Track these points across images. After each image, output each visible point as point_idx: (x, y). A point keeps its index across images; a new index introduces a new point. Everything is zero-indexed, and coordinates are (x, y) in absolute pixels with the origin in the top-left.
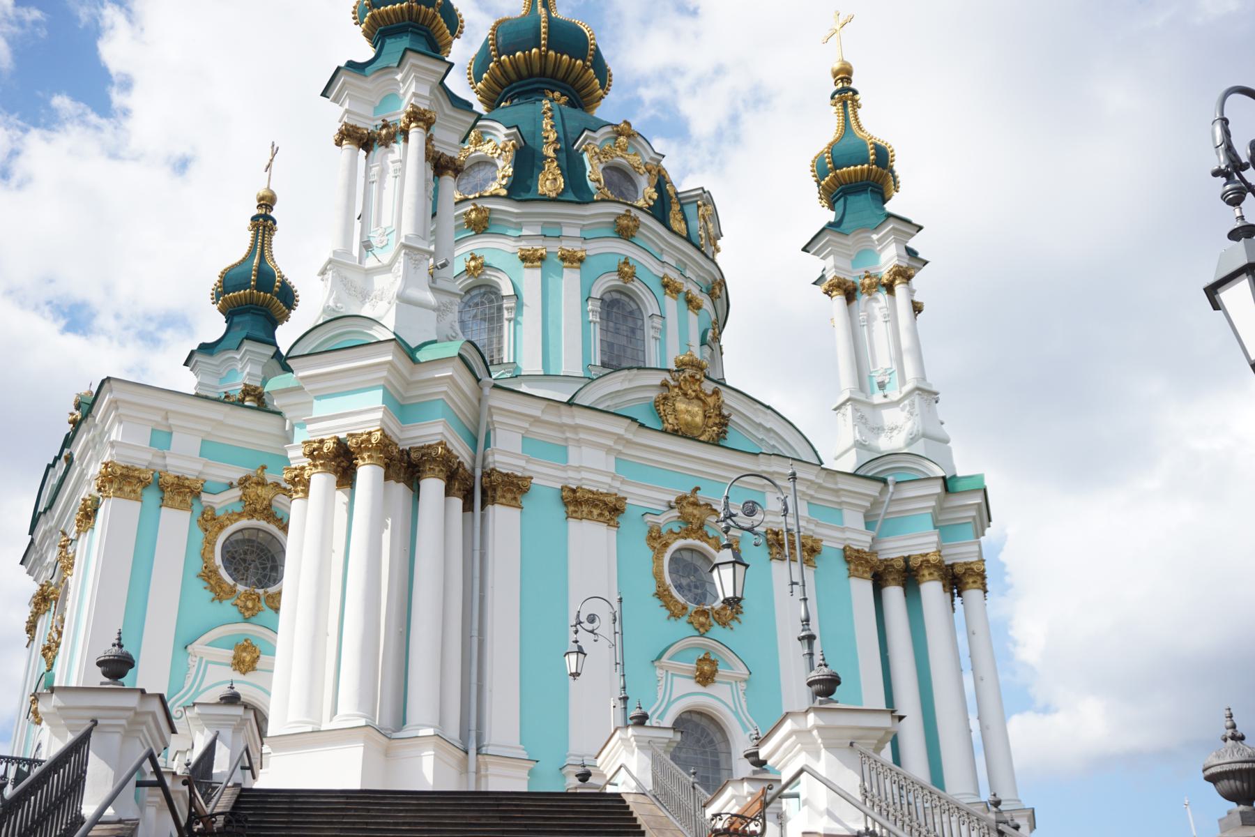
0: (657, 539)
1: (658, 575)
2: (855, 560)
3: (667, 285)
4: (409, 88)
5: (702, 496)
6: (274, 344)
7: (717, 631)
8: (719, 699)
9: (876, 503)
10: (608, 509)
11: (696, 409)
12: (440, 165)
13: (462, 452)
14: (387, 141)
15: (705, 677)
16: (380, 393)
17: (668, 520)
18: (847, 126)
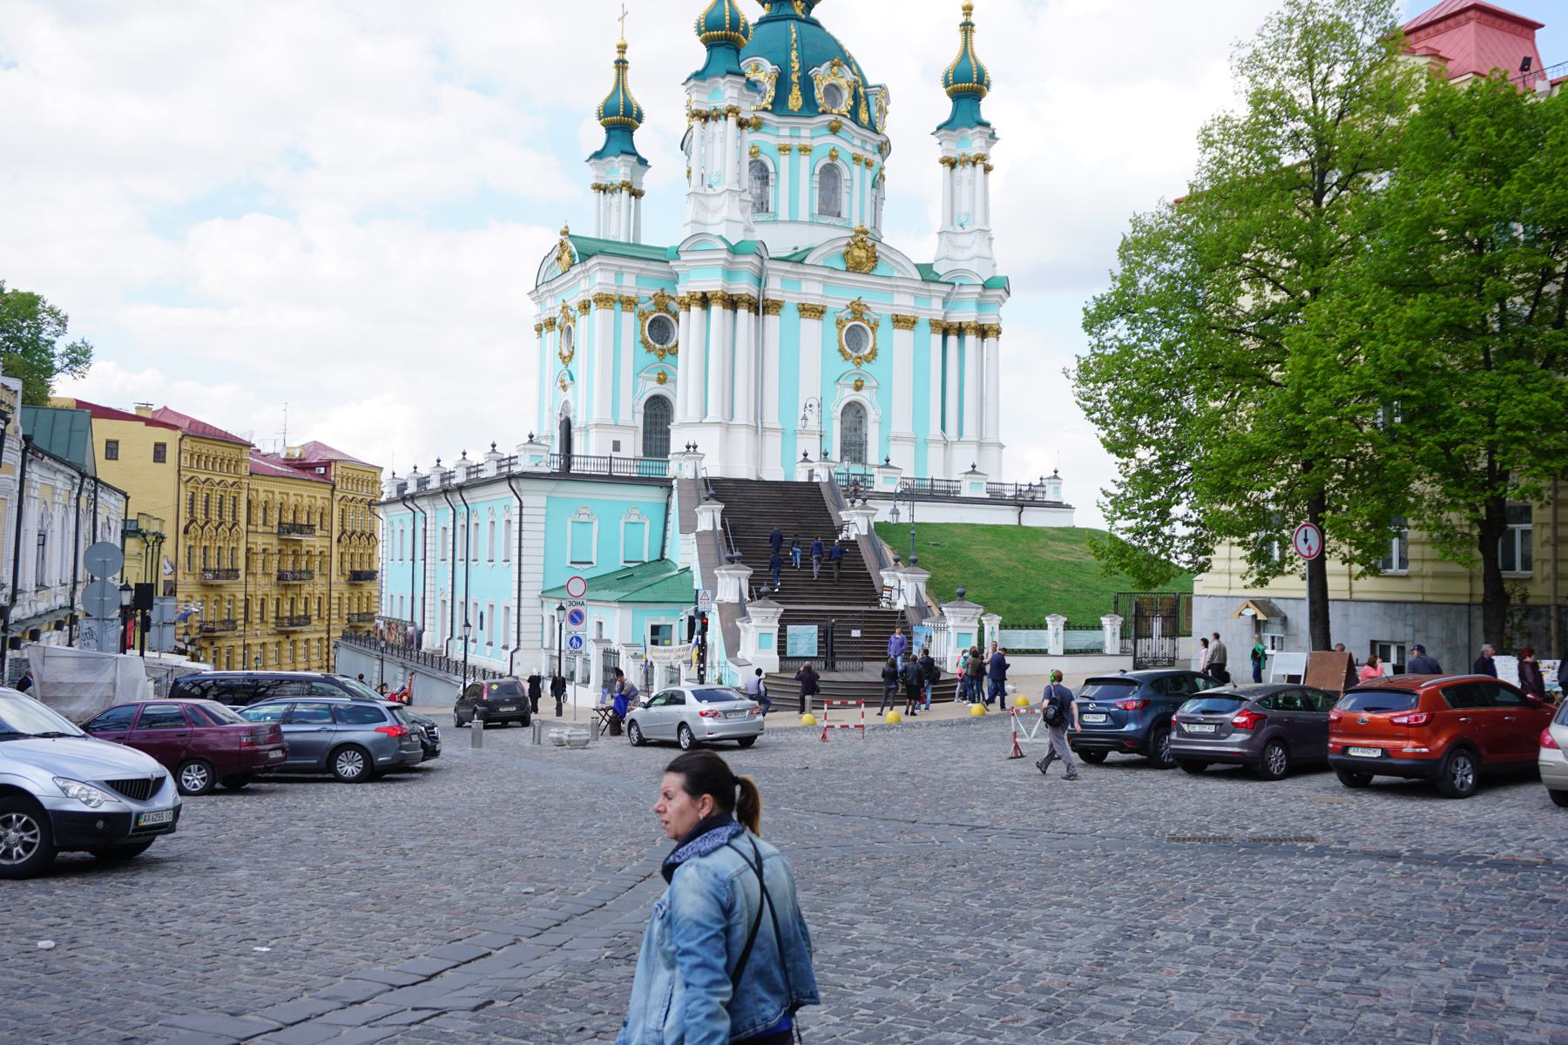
0: (839, 323)
2: (934, 325)
3: (856, 159)
4: (727, 93)
5: (863, 301)
6: (635, 154)
7: (865, 366)
8: (863, 397)
9: (949, 294)
10: (817, 312)
11: (863, 253)
12: (742, 124)
13: (754, 292)
14: (716, 118)
15: (858, 388)
16: (719, 271)
17: (846, 314)
18: (966, 52)
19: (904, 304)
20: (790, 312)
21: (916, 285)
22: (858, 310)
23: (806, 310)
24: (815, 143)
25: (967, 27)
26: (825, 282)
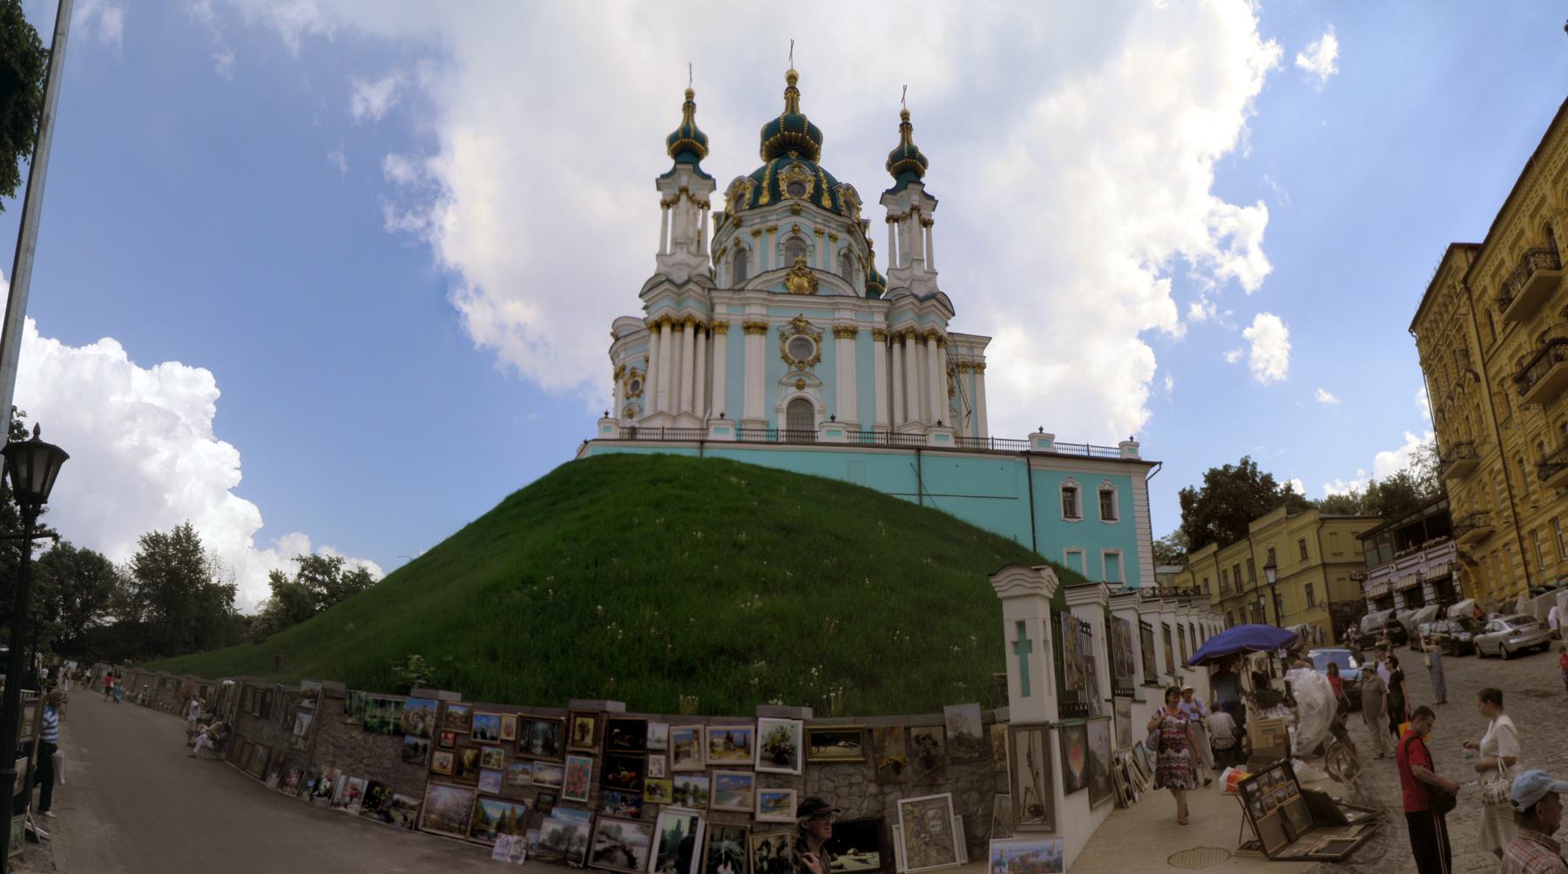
0: (783, 337)
1: (783, 351)
2: (877, 333)
3: (817, 232)
7: (808, 369)
8: (809, 393)
10: (763, 329)
15: (800, 386)
17: (788, 329)
19: (846, 317)
20: (736, 331)
21: (853, 301)
22: (798, 325)
23: (749, 328)
24: (780, 223)
25: (906, 127)
26: (766, 303)
